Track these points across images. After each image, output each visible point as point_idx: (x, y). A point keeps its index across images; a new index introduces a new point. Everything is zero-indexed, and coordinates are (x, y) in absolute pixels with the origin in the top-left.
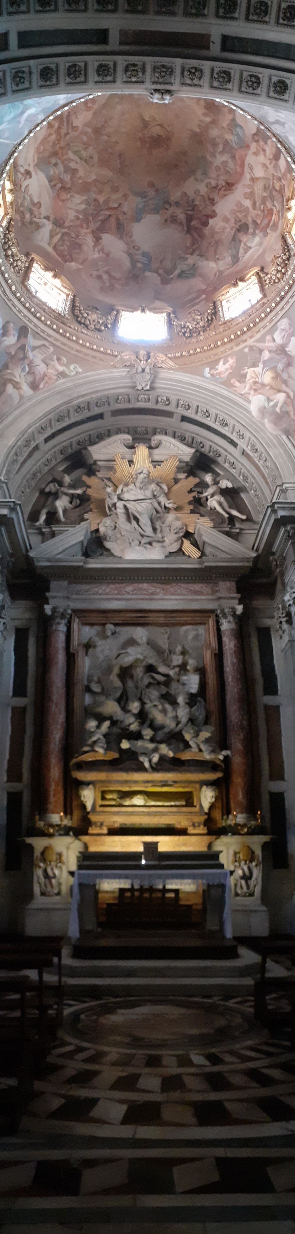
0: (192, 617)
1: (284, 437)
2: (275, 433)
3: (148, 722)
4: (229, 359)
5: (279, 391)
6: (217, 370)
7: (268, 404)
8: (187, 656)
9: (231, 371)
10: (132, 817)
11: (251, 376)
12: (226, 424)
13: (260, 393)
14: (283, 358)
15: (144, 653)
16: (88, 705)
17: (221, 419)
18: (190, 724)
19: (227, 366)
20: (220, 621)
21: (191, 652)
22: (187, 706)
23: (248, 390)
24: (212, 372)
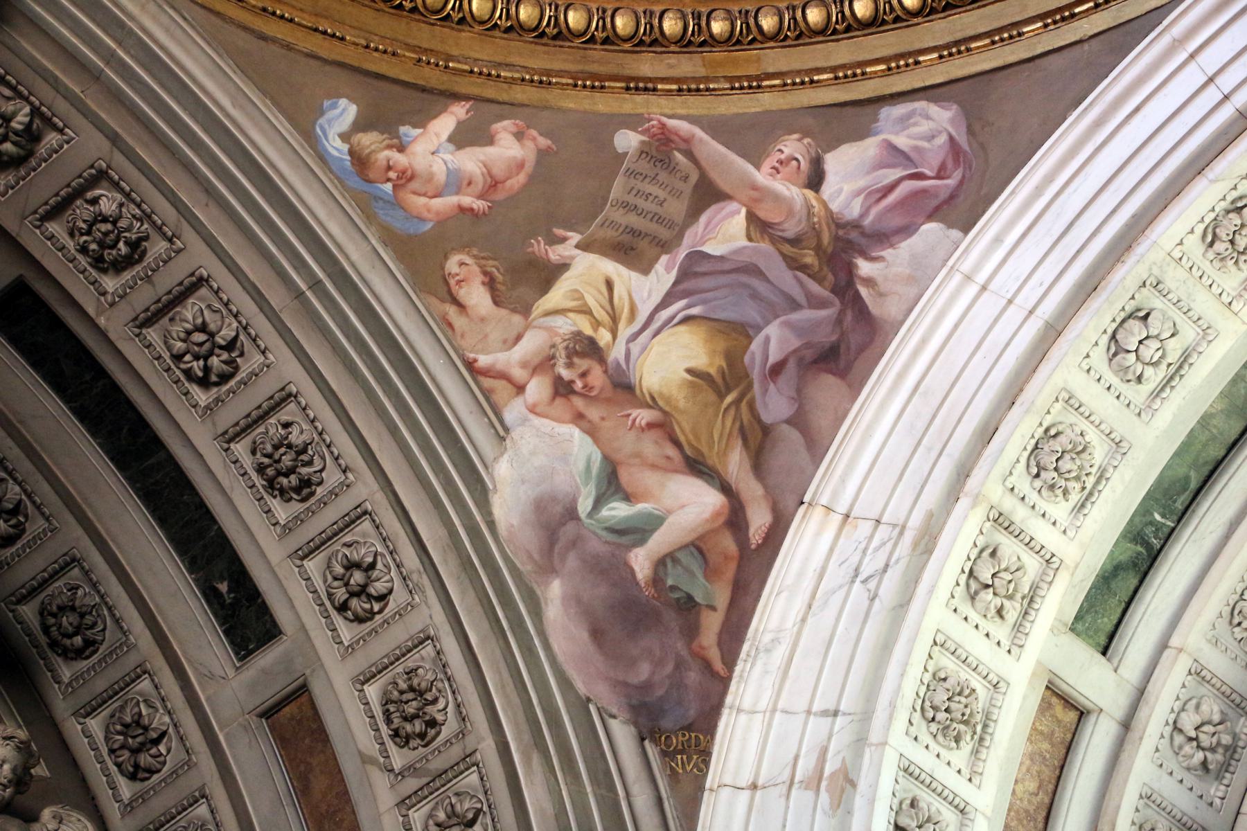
1: (623, 734)
2: (581, 688)
4: (504, 129)
5: (697, 466)
6: (401, 149)
7: (598, 503)
9: (479, 205)
11: (577, 295)
12: (305, 488)
13: (578, 418)
14: (816, 303)
17: (296, 437)
19: (471, 161)
23: (524, 365)
24: (368, 140)
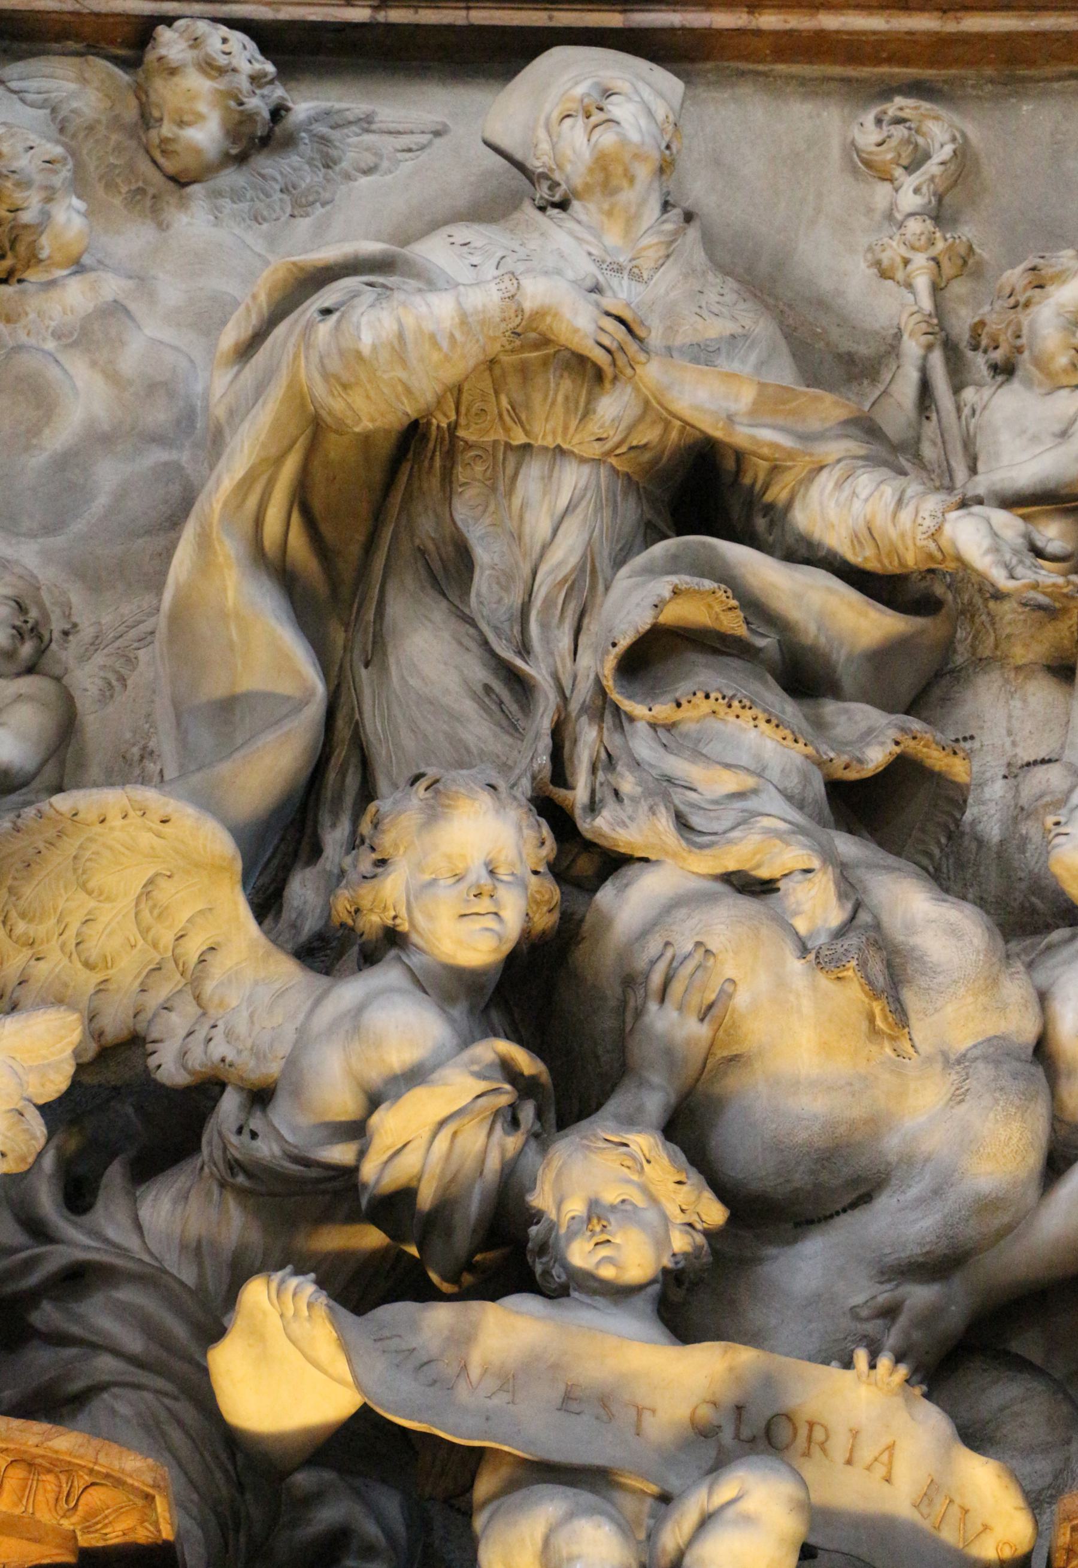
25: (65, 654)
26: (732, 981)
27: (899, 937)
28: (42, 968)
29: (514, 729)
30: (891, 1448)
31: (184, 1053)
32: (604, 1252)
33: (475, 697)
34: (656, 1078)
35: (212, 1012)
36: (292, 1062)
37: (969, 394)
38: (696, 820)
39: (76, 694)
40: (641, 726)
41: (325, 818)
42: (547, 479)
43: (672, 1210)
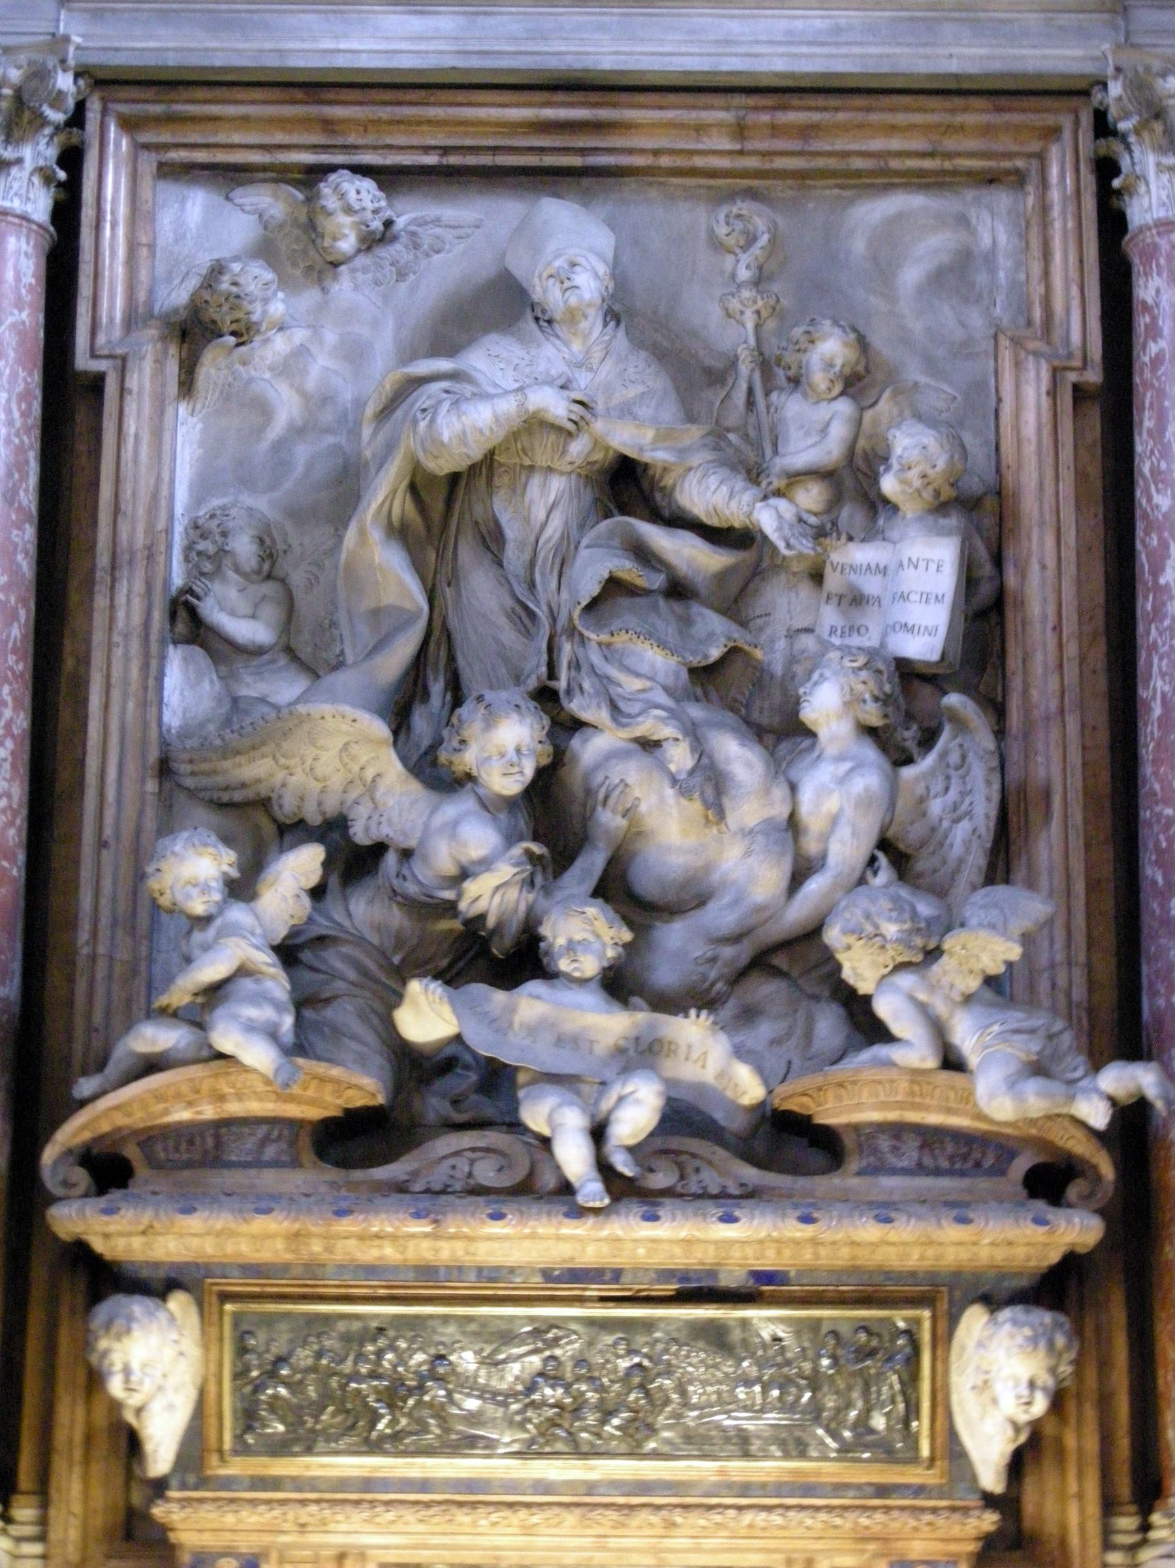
0: (927, 128)
3: (592, 863)
8: (885, 406)
10: (463, 1517)
15: (583, 380)
16: (185, 733)
18: (884, 874)
20: (1125, 163)
21: (914, 373)
22: (870, 752)
25: (285, 566)
26: (638, 799)
27: (722, 766)
28: (293, 779)
29: (527, 633)
30: (705, 1053)
31: (367, 829)
32: (575, 965)
33: (508, 617)
34: (601, 845)
35: (381, 808)
36: (422, 842)
37: (774, 396)
38: (621, 705)
39: (294, 589)
40: (594, 645)
41: (431, 677)
42: (544, 486)
43: (607, 939)
